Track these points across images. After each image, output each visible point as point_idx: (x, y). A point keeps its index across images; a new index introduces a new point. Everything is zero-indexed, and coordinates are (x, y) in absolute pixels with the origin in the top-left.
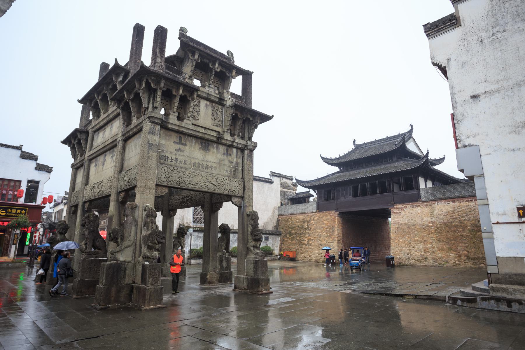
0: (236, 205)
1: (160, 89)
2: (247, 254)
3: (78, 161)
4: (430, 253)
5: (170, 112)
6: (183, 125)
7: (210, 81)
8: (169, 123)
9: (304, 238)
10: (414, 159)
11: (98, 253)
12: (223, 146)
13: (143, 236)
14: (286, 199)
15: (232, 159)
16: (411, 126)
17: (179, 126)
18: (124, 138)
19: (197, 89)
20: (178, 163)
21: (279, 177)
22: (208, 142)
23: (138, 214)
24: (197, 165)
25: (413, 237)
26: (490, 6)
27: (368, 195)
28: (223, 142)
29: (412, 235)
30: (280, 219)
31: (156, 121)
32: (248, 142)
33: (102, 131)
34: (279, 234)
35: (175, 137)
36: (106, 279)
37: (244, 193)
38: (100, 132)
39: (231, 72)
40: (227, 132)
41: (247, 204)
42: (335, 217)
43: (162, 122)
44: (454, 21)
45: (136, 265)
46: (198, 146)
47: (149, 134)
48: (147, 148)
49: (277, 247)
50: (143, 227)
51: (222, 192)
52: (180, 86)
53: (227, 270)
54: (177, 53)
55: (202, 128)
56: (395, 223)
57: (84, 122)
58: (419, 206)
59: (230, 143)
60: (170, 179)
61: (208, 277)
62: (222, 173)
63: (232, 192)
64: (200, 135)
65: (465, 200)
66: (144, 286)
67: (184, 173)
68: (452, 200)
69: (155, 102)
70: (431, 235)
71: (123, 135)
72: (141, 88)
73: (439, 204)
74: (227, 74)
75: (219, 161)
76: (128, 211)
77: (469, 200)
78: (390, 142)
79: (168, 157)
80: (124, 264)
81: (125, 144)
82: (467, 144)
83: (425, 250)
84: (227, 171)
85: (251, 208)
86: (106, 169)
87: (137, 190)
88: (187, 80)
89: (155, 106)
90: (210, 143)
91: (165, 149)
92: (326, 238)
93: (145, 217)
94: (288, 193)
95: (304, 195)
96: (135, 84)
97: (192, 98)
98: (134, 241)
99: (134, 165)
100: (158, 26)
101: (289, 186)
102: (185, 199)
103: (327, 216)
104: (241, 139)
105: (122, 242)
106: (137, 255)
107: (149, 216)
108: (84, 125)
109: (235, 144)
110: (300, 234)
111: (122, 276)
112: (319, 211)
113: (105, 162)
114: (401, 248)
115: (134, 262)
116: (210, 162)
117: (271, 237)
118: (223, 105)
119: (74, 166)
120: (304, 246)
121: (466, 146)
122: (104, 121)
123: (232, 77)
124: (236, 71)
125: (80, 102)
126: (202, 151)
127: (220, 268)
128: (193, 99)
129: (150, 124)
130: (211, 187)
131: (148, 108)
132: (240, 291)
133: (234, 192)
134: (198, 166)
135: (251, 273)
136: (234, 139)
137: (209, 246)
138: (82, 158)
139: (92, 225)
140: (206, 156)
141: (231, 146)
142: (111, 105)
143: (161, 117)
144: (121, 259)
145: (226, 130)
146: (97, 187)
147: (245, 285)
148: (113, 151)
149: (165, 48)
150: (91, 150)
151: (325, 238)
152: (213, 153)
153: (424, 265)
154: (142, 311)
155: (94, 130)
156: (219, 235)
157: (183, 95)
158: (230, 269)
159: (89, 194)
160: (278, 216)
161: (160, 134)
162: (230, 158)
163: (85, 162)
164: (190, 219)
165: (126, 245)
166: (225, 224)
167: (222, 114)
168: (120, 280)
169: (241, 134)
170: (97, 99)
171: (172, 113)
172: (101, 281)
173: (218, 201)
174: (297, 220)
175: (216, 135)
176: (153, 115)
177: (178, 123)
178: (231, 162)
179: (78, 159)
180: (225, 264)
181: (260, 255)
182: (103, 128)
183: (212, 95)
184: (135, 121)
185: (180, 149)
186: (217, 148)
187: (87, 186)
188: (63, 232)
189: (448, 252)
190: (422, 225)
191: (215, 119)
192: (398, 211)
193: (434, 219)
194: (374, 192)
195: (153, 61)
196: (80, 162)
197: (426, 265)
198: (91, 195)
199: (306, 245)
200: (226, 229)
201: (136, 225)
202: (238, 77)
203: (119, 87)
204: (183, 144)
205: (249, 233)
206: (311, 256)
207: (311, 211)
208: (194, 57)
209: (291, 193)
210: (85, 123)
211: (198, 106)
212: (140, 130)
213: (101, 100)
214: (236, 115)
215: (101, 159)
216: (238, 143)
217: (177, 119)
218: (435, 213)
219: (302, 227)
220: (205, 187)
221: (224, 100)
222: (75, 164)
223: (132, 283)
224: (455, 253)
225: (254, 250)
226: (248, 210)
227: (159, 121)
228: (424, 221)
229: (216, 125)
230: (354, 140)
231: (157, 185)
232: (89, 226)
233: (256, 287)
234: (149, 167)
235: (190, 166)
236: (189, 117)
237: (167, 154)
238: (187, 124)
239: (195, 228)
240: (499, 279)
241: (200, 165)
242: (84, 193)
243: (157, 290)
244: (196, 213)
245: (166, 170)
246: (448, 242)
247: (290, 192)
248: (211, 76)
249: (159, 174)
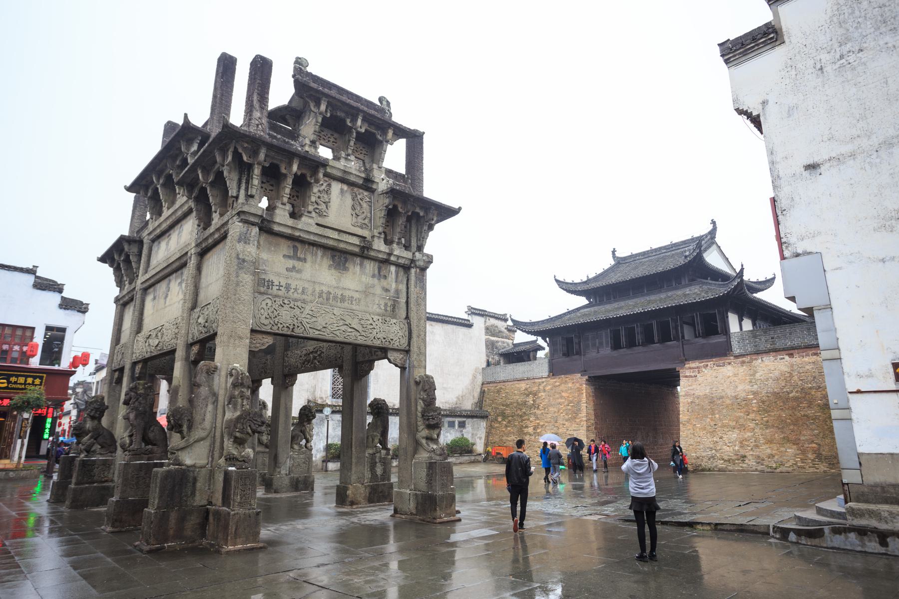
0: (396, 365)
1: (259, 164)
2: (415, 452)
3: (125, 292)
4: (750, 448)
5: (277, 204)
6: (299, 227)
7: (347, 148)
8: (274, 222)
9: (528, 422)
10: (718, 281)
11: (151, 452)
12: (372, 262)
13: (227, 421)
14: (496, 354)
15: (388, 284)
16: (714, 223)
17: (292, 228)
18: (199, 250)
19: (324, 164)
20: (290, 293)
21: (482, 315)
22: (345, 255)
23: (219, 383)
24: (325, 296)
25: (720, 420)
26: (835, 8)
27: (639, 345)
28: (372, 254)
29: (717, 416)
30: (486, 389)
31: (252, 219)
32: (417, 254)
33: (165, 239)
34: (484, 417)
35: (285, 247)
36: (160, 497)
37: (409, 344)
38: (163, 240)
39: (385, 133)
40: (379, 237)
41: (415, 363)
42: (581, 385)
43: (262, 221)
44: (772, 36)
45: (214, 473)
46: (327, 262)
47: (239, 242)
48: (236, 267)
49: (480, 438)
50: (227, 405)
51: (369, 343)
52: (294, 158)
53: (383, 481)
54: (290, 102)
55: (334, 232)
56: (687, 395)
57: (138, 225)
58: (729, 364)
59: (385, 257)
60: (276, 320)
61: (349, 492)
62: (370, 310)
63: (388, 343)
64: (331, 243)
65: (811, 353)
66: (227, 509)
67: (302, 310)
68: (787, 352)
69: (250, 186)
70: (752, 416)
71: (197, 246)
72: (226, 163)
73: (764, 359)
74: (379, 137)
75: (365, 288)
76: (201, 378)
78: (676, 251)
79: (272, 282)
80: (193, 472)
81: (201, 260)
82: (800, 251)
83: (741, 443)
84: (379, 305)
85: (423, 370)
86: (170, 305)
87: (218, 340)
88: (307, 148)
89: (249, 194)
90: (348, 256)
91: (267, 269)
92: (567, 423)
93: (230, 388)
94: (500, 344)
95: (528, 346)
96: (215, 157)
97: (315, 179)
98: (212, 430)
99: (215, 296)
100: (256, 56)
101: (500, 332)
102: (311, 355)
103: (568, 383)
104: (403, 249)
105: (190, 432)
106: (216, 455)
107: (237, 386)
108: (137, 230)
109: (392, 258)
110: (521, 416)
111: (189, 493)
112: (553, 375)
113: (169, 293)
114: (699, 439)
115: (211, 467)
116: (350, 290)
117: (469, 422)
118: (372, 191)
119: (119, 300)
121: (798, 255)
122: (169, 222)
123: (387, 142)
124: (394, 130)
125: (129, 189)
126: (333, 271)
127: (370, 476)
128: (317, 181)
129: (240, 224)
130: (350, 334)
131: (237, 197)
132: (404, 517)
133: (392, 343)
134: (327, 298)
135: (423, 485)
136: (392, 250)
137: (352, 439)
138: (132, 287)
139: (142, 402)
140: (342, 279)
141: (386, 262)
142: (179, 194)
143: (260, 213)
144: (188, 461)
145: (377, 234)
146: (154, 336)
147: (412, 506)
148: (182, 273)
149: (268, 93)
150: (146, 272)
151: (564, 422)
152: (354, 273)
153: (741, 469)
154: (221, 554)
155: (151, 237)
156: (369, 419)
157: (299, 173)
158: (389, 479)
159: (142, 348)
160: (482, 384)
161: (258, 242)
162: (384, 283)
163: (137, 292)
164: (326, 391)
165: (197, 437)
166: (380, 400)
167: (371, 206)
168: (184, 498)
169: (403, 240)
170: (156, 185)
171: (280, 206)
172: (151, 501)
173: (367, 358)
174: (515, 390)
175: (358, 243)
176: (246, 208)
177: (290, 222)
178: (387, 290)
179: (126, 287)
180: (379, 470)
181: (438, 452)
182: (168, 234)
183: (351, 173)
184: (216, 221)
185: (294, 267)
186: (361, 265)
187: (139, 335)
188: (97, 415)
189: (782, 445)
190: (736, 397)
191: (358, 216)
192: (692, 374)
193: (755, 386)
194: (649, 340)
195: (246, 115)
196: (129, 293)
197: (744, 469)
198: (145, 349)
199: (530, 435)
200: (381, 408)
201: (216, 402)
202: (400, 140)
203: (191, 161)
204: (299, 259)
205: (419, 414)
207: (540, 375)
208: (319, 108)
209: (505, 345)
210: (138, 226)
211: (328, 192)
212: (224, 237)
213: (163, 185)
214: (395, 207)
215: (162, 287)
216: (398, 257)
217: (288, 215)
218: (758, 376)
219: (525, 403)
220: (339, 334)
221: (373, 182)
222: (121, 296)
223: (207, 505)
224: (795, 447)
225: (428, 445)
226: (417, 374)
227: (256, 220)
228: (738, 390)
229: (359, 225)
230: (614, 249)
231: (253, 331)
232: (137, 403)
233: (431, 510)
234: (239, 300)
235: (313, 298)
236: (310, 212)
237: (271, 277)
238: (307, 224)
239: (336, 406)
240: (863, 494)
241: (331, 296)
242: (135, 347)
243: (250, 517)
244: (336, 380)
245: (269, 305)
246: (783, 428)
247: (503, 342)
248: (349, 141)
249: (257, 311)
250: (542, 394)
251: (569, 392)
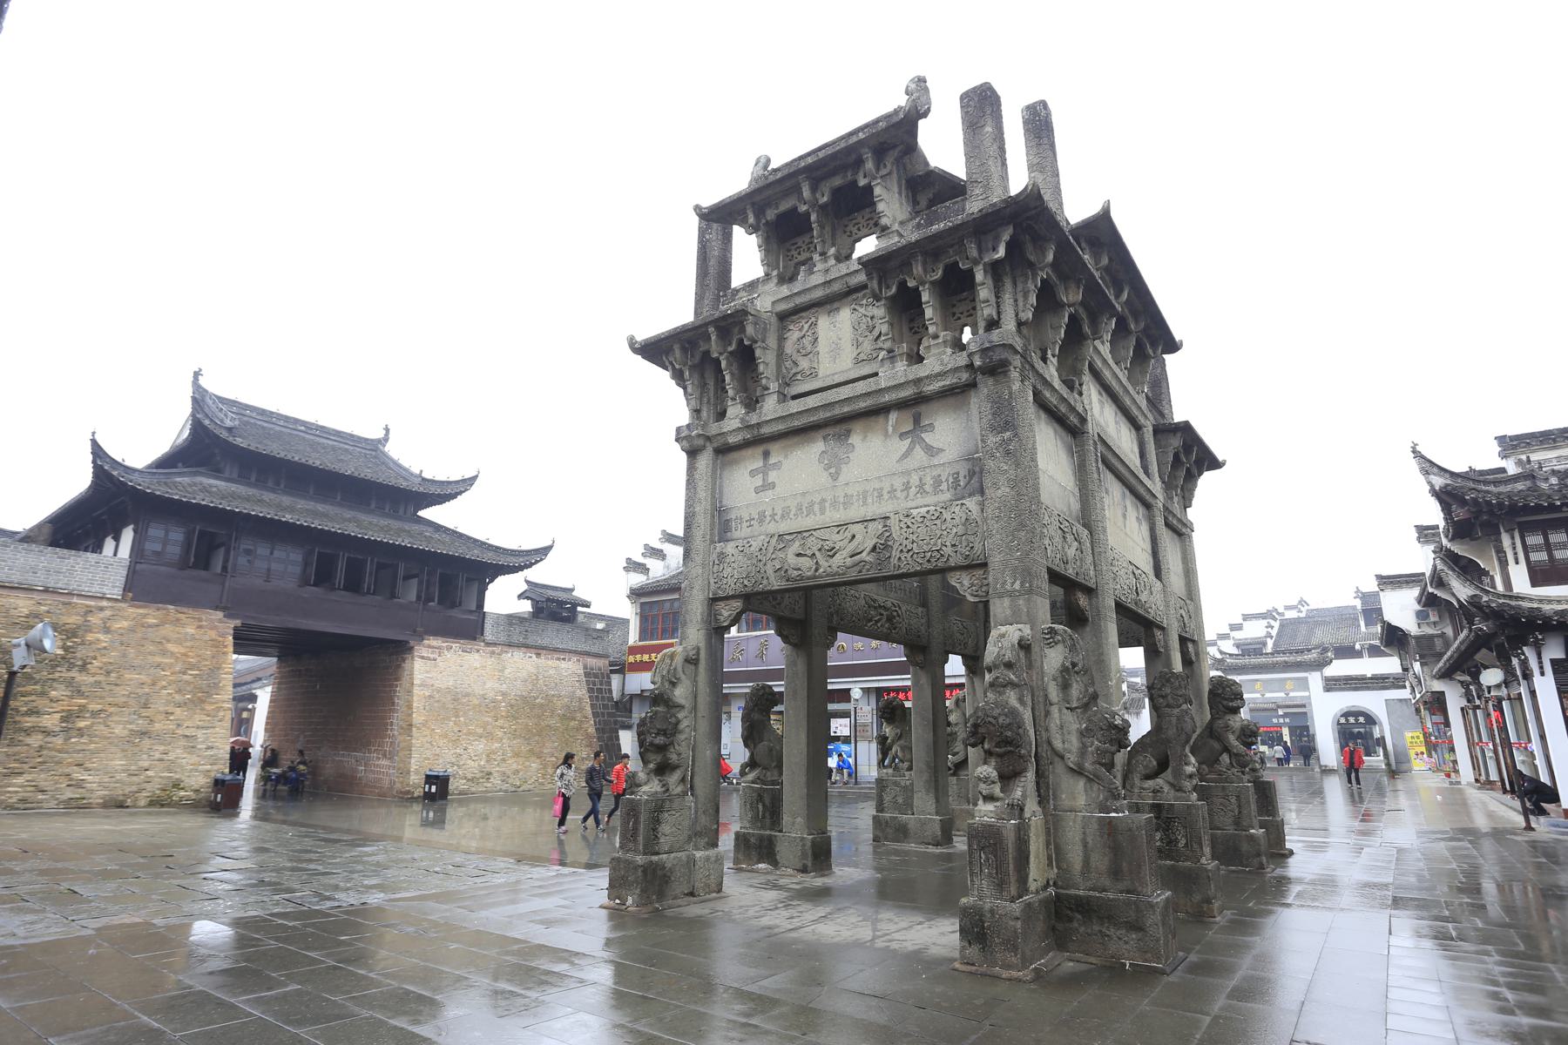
4: (496, 763)
9: (41, 703)
10: (176, 468)
16: (387, 430)
27: (339, 589)
29: (462, 719)
42: (223, 635)
65: (556, 656)
68: (536, 651)
77: (562, 657)
83: (488, 756)
92: (178, 711)
103: (183, 625)
112: (132, 599)
120: (35, 740)
153: (485, 789)
190: (484, 697)
192: (429, 655)
199: (47, 732)
206: (79, 784)
207: (95, 589)
218: (507, 672)
224: (538, 761)
230: (200, 370)
246: (529, 739)
250: (101, 636)
251: (188, 644)
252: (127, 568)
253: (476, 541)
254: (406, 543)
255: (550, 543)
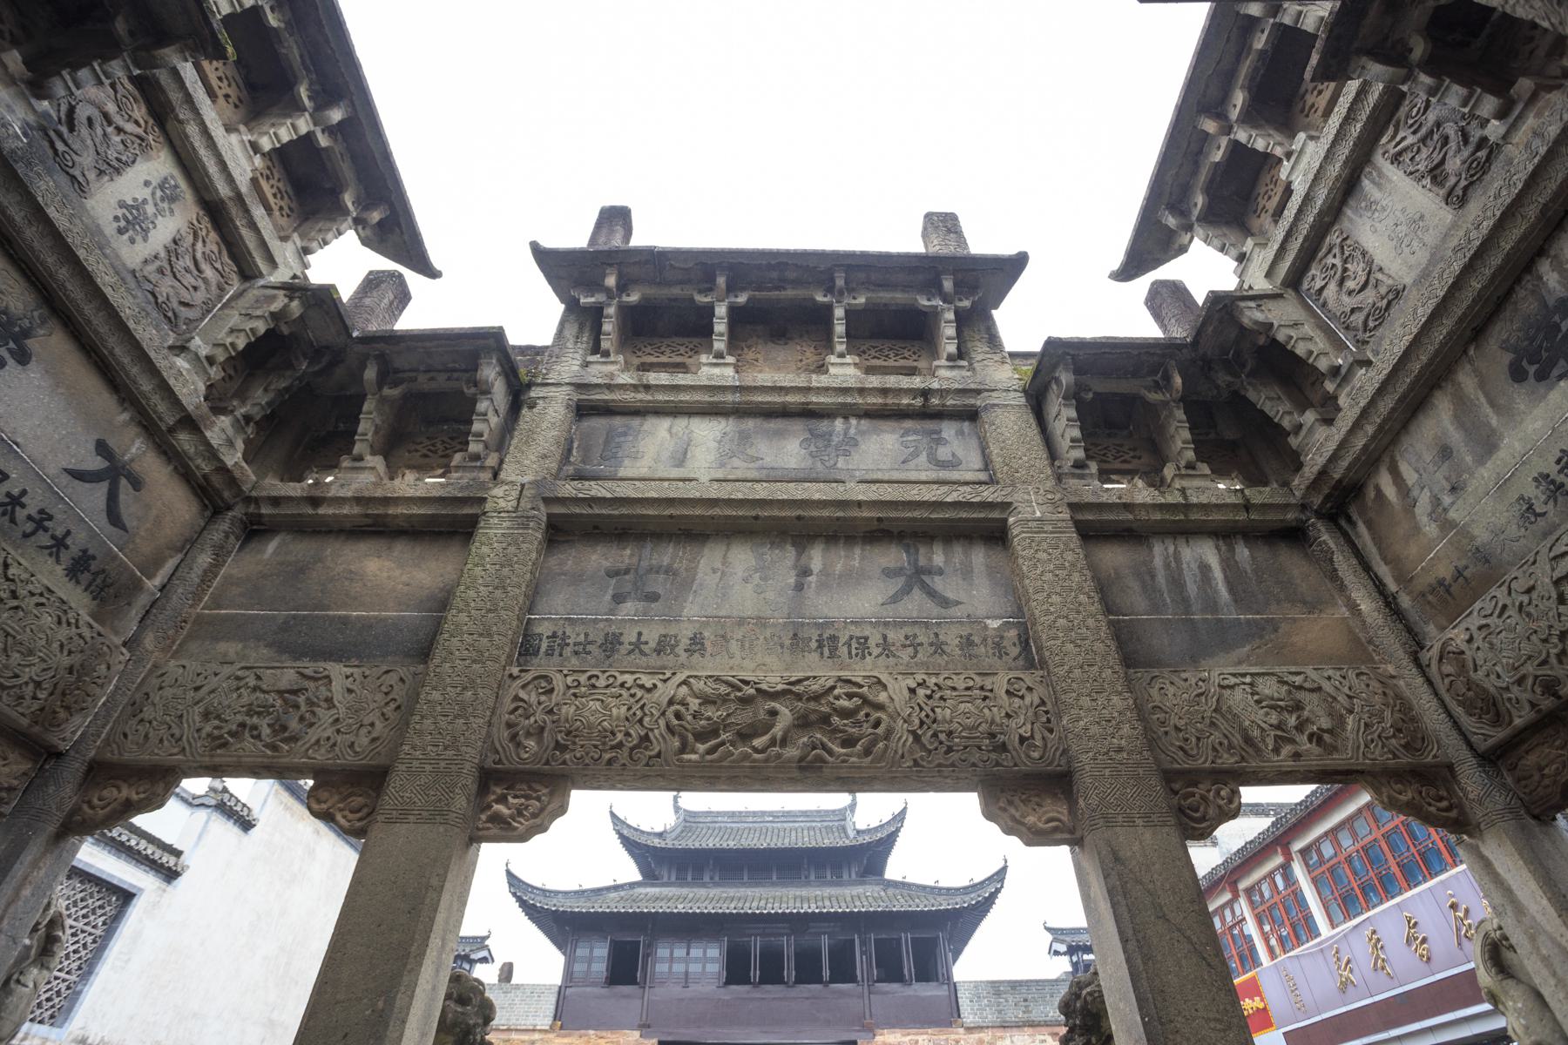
68: (1050, 1029)
73: (1015, 1039)
112: (561, 1028)
207: (528, 1023)
252: (556, 995)
253: (924, 888)
254: (813, 909)
255: (1001, 864)
